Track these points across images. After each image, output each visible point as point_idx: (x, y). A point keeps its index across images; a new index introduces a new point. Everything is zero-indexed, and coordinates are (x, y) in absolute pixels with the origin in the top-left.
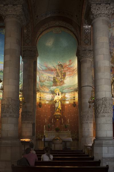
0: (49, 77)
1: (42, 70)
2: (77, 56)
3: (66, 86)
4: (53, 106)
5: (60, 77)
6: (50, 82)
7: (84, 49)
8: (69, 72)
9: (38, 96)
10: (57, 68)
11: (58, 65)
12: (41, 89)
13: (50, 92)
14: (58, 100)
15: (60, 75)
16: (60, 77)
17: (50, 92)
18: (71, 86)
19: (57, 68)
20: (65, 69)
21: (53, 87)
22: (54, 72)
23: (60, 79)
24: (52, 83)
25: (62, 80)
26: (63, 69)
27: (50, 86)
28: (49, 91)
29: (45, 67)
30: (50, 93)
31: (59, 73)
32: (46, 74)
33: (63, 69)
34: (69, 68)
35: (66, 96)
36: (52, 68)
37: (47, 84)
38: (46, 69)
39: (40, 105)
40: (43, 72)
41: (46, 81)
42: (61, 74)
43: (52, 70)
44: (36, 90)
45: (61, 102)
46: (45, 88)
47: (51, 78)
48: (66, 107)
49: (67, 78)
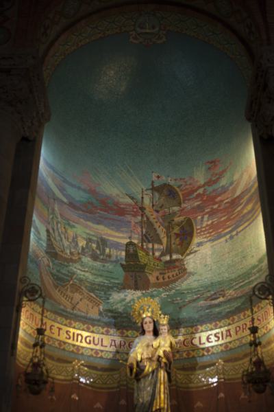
0: (103, 242)
1: (65, 200)
2: (249, 120)
3: (195, 285)
4: (123, 402)
5: (161, 243)
6: (110, 266)
8: (212, 213)
9: (26, 326)
10: (147, 201)
11: (154, 189)
12: (56, 294)
13: (106, 319)
14: (150, 359)
15: (163, 235)
16: (161, 243)
17: (106, 319)
18: (220, 283)
19: (147, 201)
20: (187, 205)
21: (122, 295)
22: (129, 218)
23: (163, 254)
24: (120, 273)
25: (174, 257)
26: (180, 204)
27: (109, 288)
28: (100, 314)
29: (82, 193)
30: (107, 325)
31: (156, 226)
32: (86, 227)
33: (180, 204)
34: (211, 199)
35: (196, 342)
36: (121, 200)
37: (87, 274)
38: (92, 204)
39: (36, 379)
40: (72, 214)
41: (86, 259)
42: (169, 228)
43: (121, 211)
44: (20, 286)
45: (169, 374)
46: (77, 296)
47: (116, 246)
48: (199, 404)
49: (200, 244)
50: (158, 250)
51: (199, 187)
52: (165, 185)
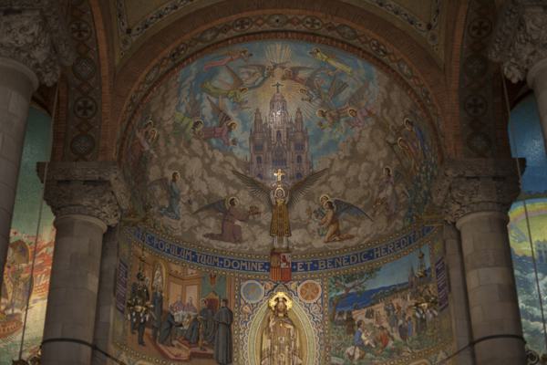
7: (60, 178)
50: (5, 303)
51: (44, 246)
52: (20, 241)
